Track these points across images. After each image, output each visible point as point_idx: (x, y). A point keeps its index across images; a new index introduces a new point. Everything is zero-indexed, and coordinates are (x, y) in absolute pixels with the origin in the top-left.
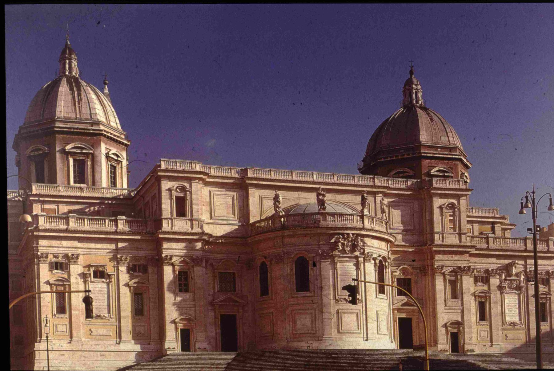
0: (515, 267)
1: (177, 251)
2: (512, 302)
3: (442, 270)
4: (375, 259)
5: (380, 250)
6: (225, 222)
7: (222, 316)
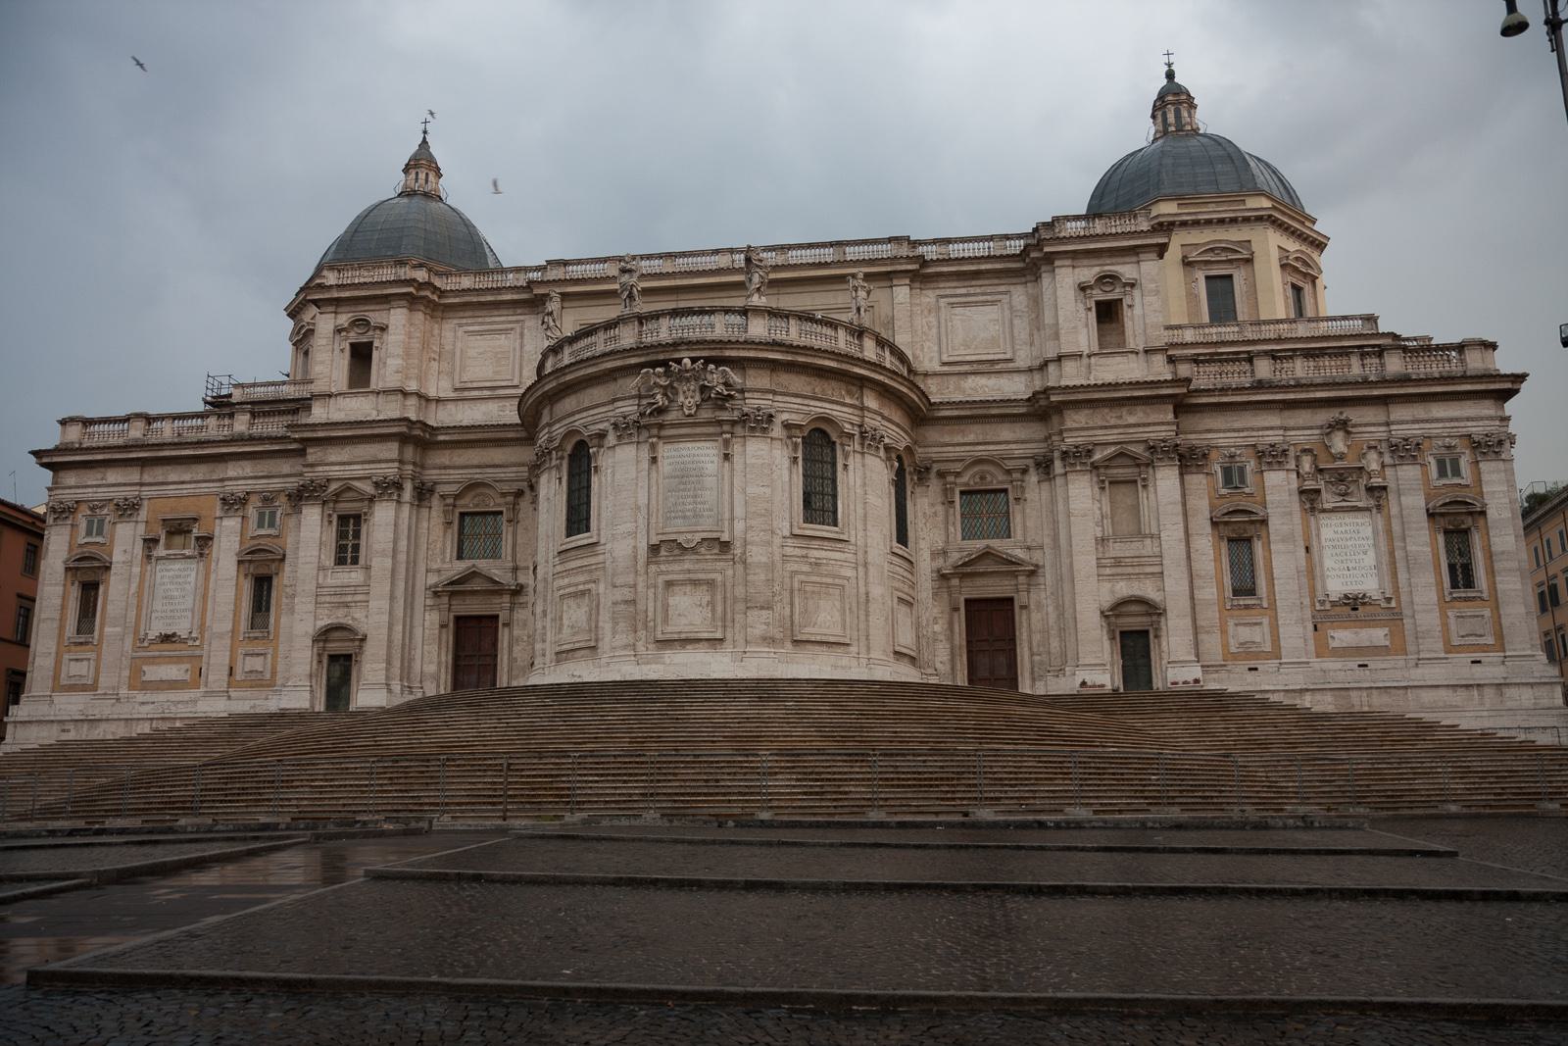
0: (1348, 433)
1: (337, 468)
2: (1349, 536)
3: (1090, 457)
4: (787, 426)
5: (812, 403)
6: (487, 393)
7: (459, 620)
